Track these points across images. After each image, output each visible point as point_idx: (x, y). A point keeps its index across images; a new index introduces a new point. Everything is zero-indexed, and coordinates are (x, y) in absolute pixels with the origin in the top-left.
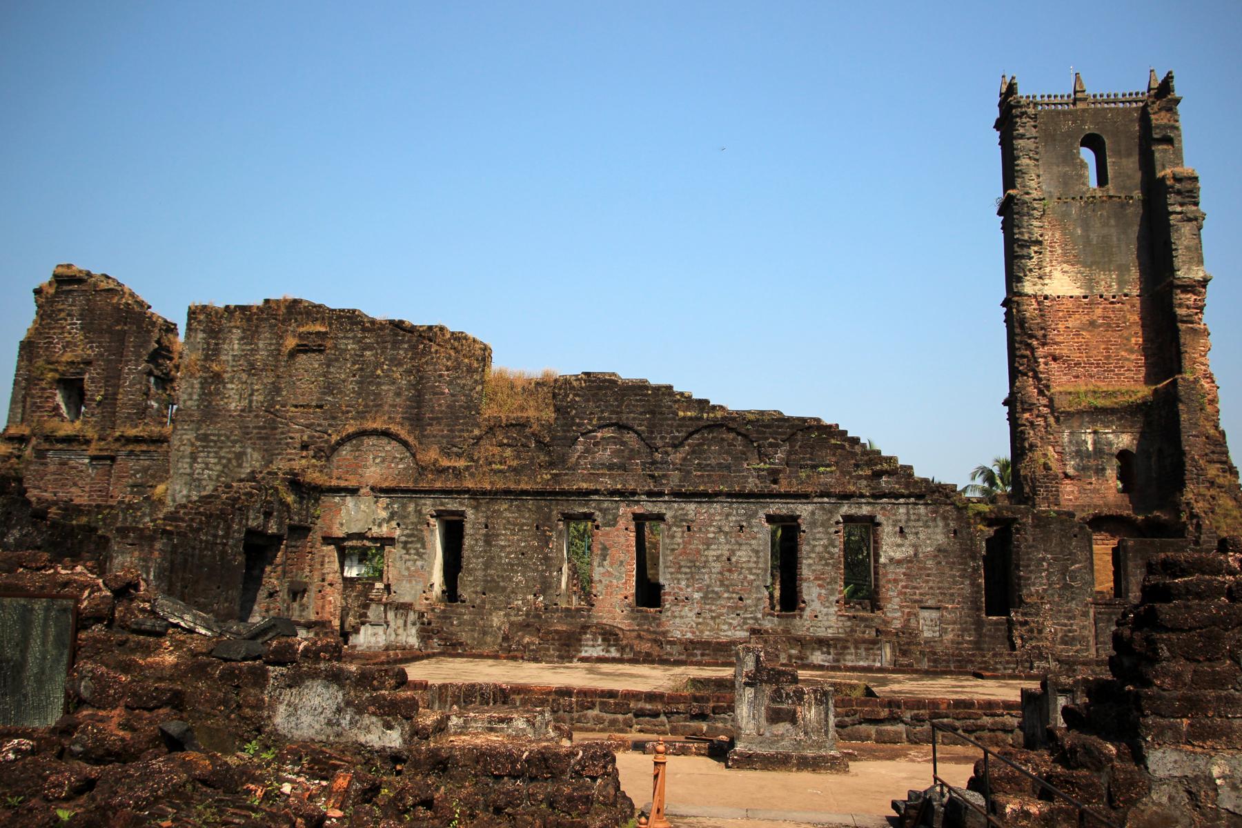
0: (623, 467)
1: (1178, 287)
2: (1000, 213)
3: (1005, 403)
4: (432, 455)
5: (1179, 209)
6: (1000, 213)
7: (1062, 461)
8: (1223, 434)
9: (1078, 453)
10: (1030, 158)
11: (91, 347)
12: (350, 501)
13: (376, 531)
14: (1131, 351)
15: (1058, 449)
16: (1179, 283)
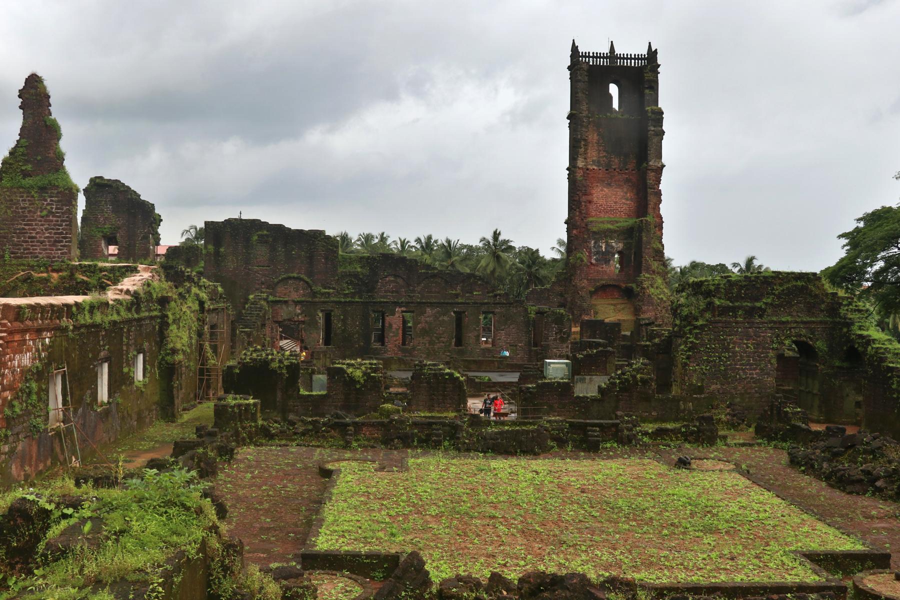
0: (397, 292)
1: (649, 170)
2: (568, 118)
3: (565, 223)
4: (319, 288)
5: (653, 129)
6: (568, 118)
7: (590, 257)
8: (663, 246)
9: (597, 253)
10: (583, 93)
11: (119, 220)
12: (284, 307)
13: (296, 319)
14: (627, 200)
15: (588, 250)
16: (650, 168)
